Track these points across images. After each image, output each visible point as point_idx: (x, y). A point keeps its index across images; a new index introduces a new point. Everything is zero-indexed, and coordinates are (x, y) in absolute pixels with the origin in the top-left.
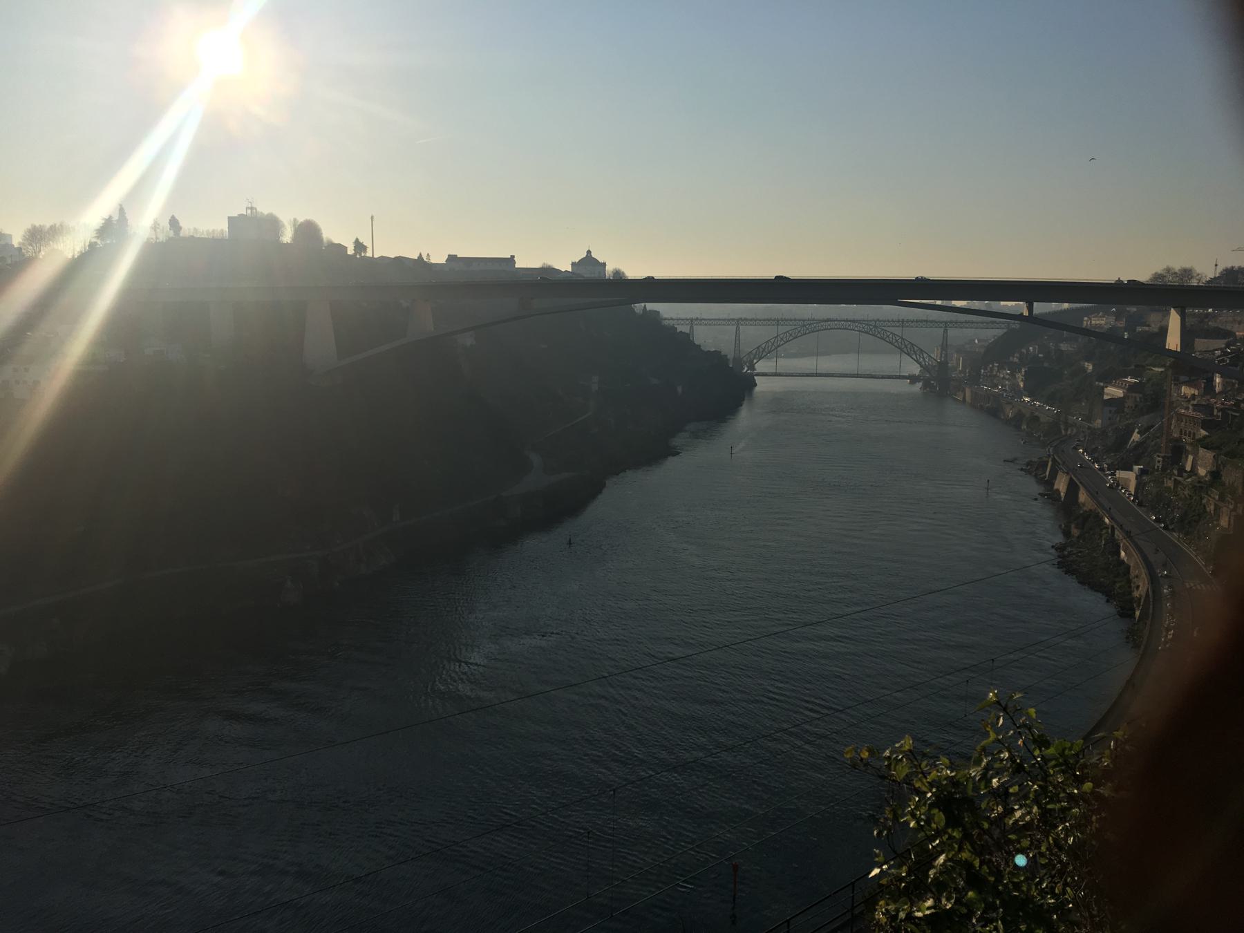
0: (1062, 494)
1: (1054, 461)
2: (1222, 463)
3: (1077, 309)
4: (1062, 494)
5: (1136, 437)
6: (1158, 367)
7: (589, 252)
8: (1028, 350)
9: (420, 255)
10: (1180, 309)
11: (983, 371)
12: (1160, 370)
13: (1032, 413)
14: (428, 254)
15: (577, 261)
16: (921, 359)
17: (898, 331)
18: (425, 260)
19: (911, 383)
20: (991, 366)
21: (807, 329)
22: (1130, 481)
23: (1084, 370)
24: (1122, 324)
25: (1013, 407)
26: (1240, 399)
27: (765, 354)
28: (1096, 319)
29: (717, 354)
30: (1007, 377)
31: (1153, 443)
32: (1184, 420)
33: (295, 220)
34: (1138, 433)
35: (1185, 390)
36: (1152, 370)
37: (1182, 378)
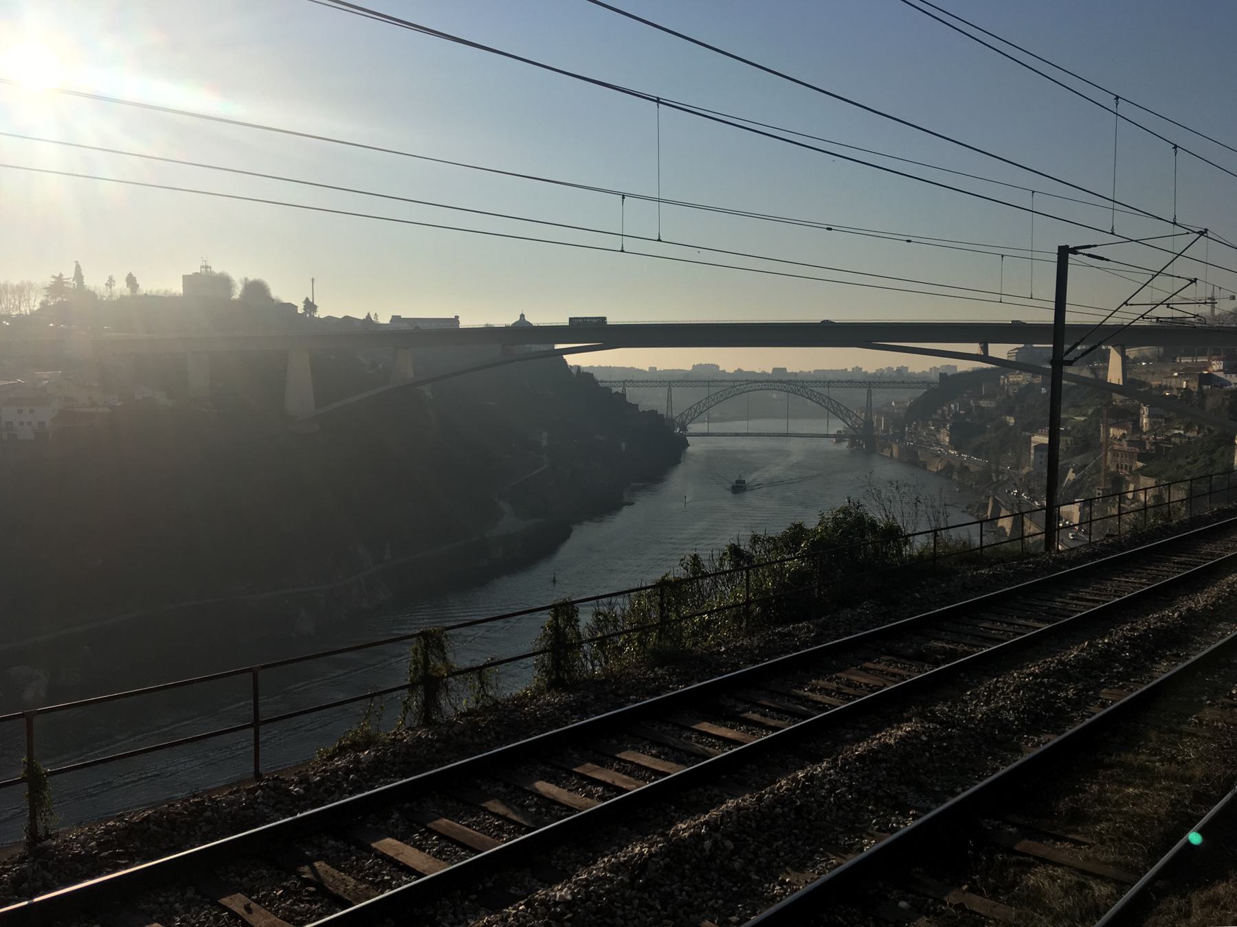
0: (1008, 530)
1: (995, 501)
4: (1008, 530)
6: (1080, 416)
7: (522, 316)
8: (950, 408)
9: (369, 315)
11: (907, 429)
12: (1082, 419)
13: (962, 464)
14: (376, 314)
18: (373, 319)
19: (838, 442)
20: (915, 423)
22: (1073, 513)
23: (1006, 424)
25: (942, 459)
26: (1169, 435)
27: (696, 414)
28: (1013, 376)
29: (653, 413)
31: (1090, 479)
32: (1120, 455)
33: (246, 279)
34: (1073, 472)
37: (1111, 421)
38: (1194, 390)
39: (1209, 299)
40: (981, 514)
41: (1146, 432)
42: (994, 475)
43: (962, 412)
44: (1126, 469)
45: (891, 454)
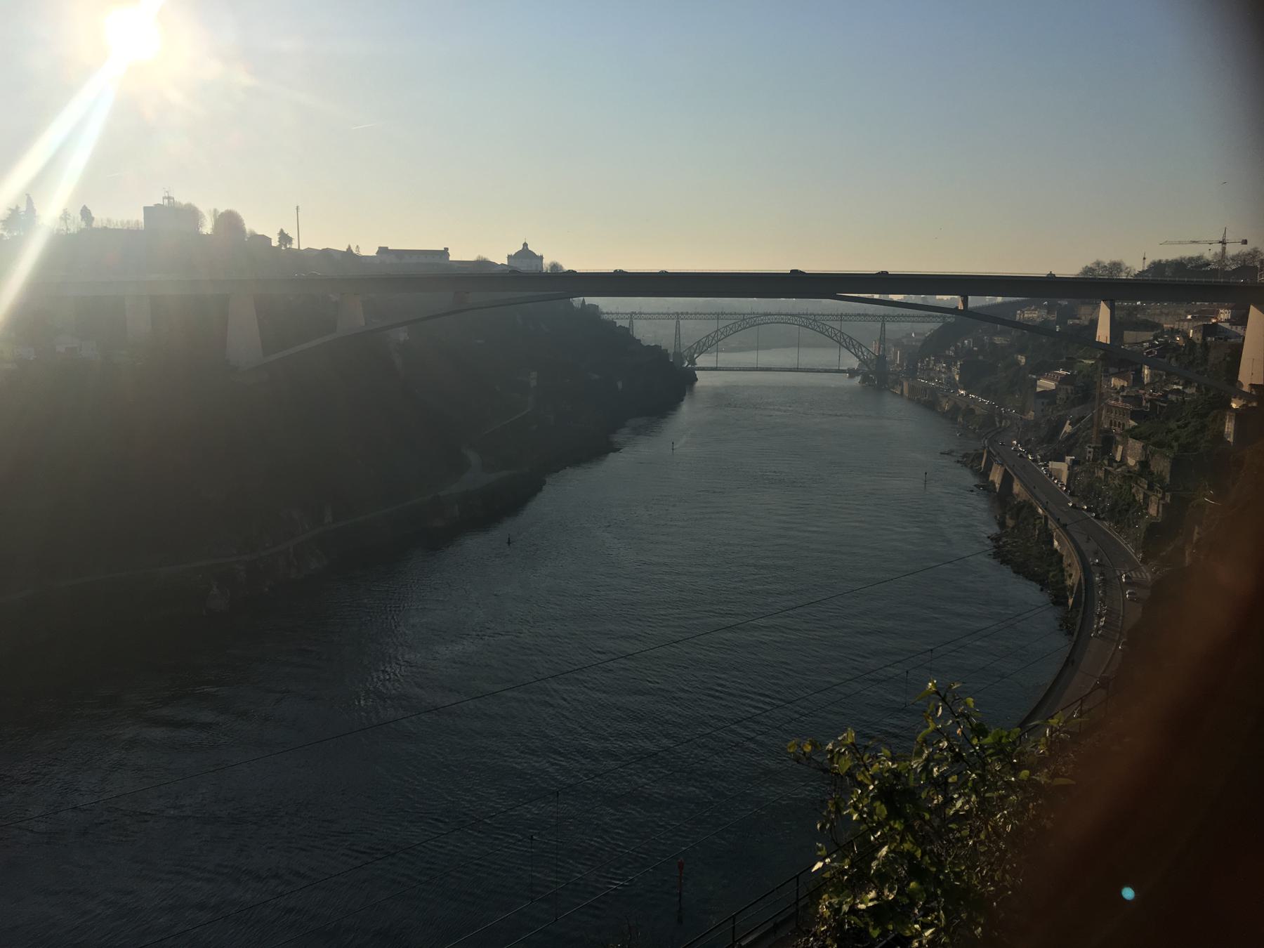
0: (997, 486)
1: (989, 452)
2: (1150, 452)
3: (1011, 303)
5: (1068, 428)
6: (1090, 359)
7: (525, 245)
8: (963, 343)
9: (349, 247)
10: (1109, 302)
12: (1091, 362)
14: (357, 246)
15: (513, 254)
16: (860, 353)
17: (836, 325)
18: (354, 252)
21: (747, 323)
22: (1062, 471)
23: (1018, 363)
24: (1053, 317)
25: (949, 400)
27: (705, 348)
28: (1029, 312)
29: (657, 348)
30: (943, 370)
31: (1084, 434)
33: (215, 211)
35: (1116, 382)
36: (1083, 362)
37: (1112, 370)
38: (1197, 342)
39: (1220, 242)
40: (975, 465)
41: (1147, 384)
42: (997, 419)
43: (975, 349)
44: (1119, 427)
45: (902, 391)
